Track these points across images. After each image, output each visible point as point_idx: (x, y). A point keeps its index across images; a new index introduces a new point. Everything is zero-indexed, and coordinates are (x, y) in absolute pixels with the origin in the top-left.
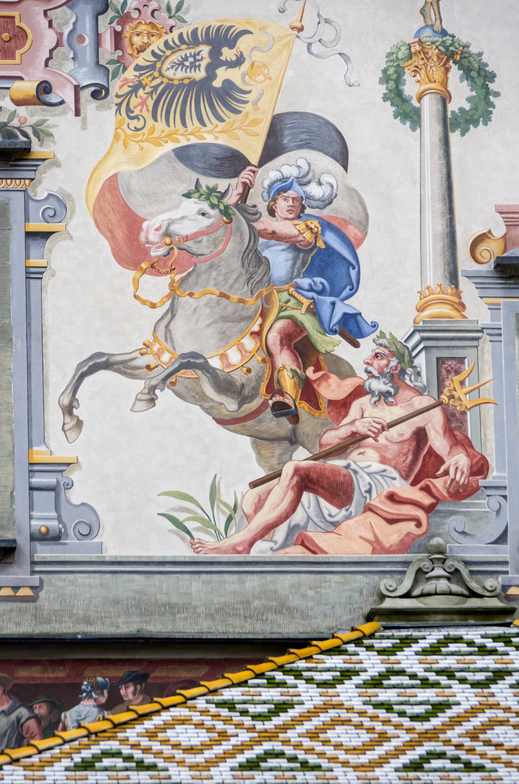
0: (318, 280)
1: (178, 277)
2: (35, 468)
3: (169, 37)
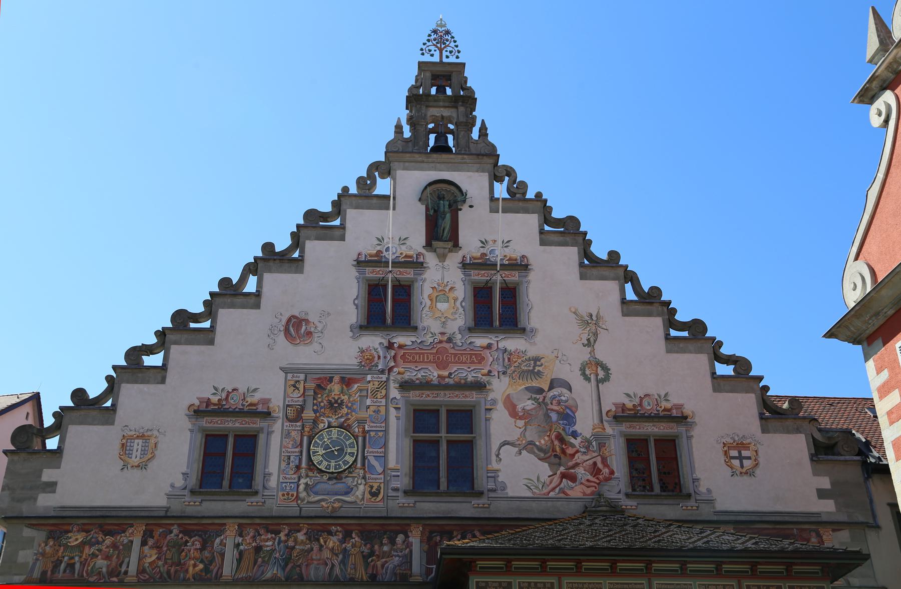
3: (523, 359)
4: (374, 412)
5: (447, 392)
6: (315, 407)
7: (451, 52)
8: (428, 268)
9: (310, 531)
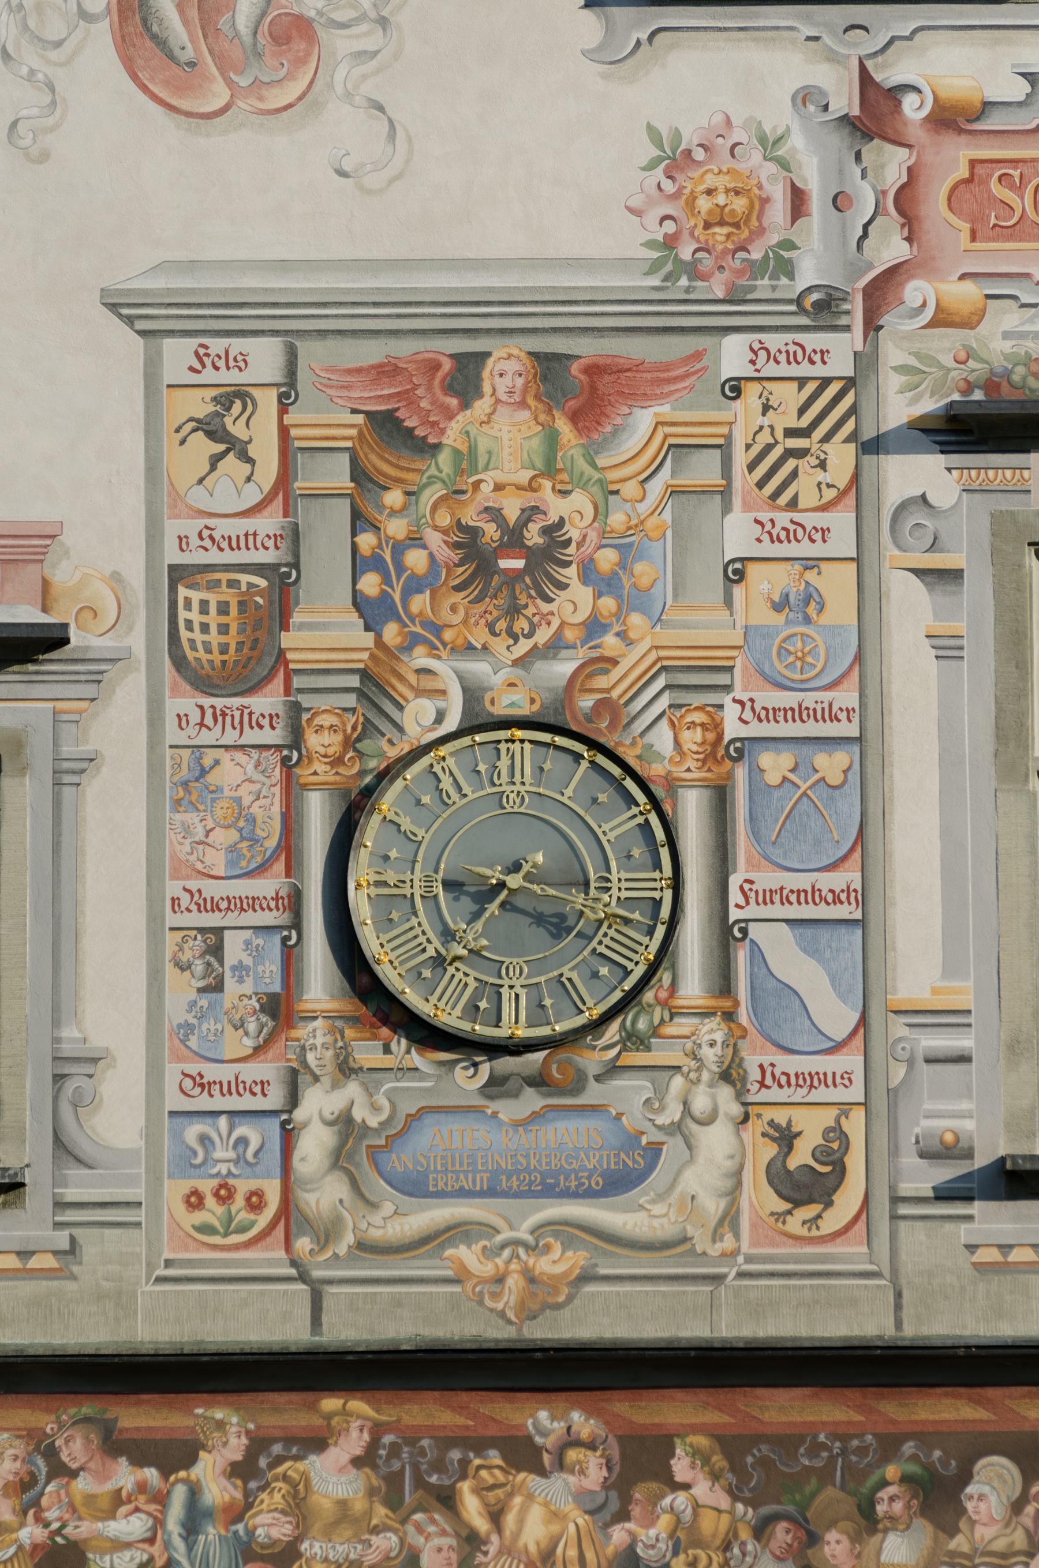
4: (778, 607)
6: (370, 584)
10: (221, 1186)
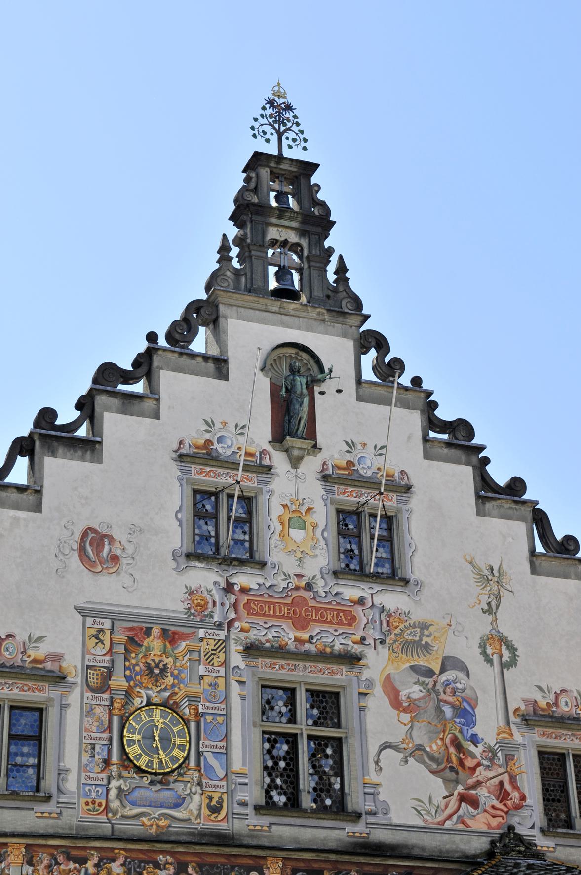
0: (462, 720)
1: (413, 715)
2: (366, 785)
3: (405, 624)
4: (210, 685)
5: (307, 664)
7: (294, 140)
8: (276, 474)
9: (129, 860)
10: (93, 801)
